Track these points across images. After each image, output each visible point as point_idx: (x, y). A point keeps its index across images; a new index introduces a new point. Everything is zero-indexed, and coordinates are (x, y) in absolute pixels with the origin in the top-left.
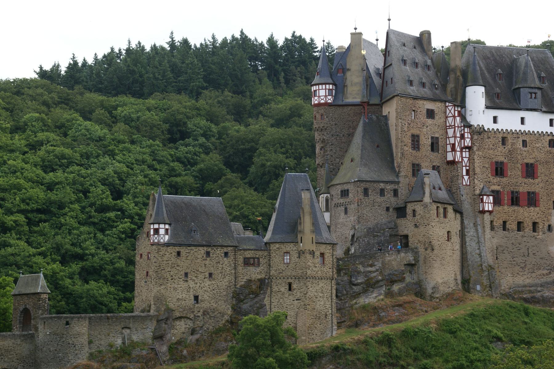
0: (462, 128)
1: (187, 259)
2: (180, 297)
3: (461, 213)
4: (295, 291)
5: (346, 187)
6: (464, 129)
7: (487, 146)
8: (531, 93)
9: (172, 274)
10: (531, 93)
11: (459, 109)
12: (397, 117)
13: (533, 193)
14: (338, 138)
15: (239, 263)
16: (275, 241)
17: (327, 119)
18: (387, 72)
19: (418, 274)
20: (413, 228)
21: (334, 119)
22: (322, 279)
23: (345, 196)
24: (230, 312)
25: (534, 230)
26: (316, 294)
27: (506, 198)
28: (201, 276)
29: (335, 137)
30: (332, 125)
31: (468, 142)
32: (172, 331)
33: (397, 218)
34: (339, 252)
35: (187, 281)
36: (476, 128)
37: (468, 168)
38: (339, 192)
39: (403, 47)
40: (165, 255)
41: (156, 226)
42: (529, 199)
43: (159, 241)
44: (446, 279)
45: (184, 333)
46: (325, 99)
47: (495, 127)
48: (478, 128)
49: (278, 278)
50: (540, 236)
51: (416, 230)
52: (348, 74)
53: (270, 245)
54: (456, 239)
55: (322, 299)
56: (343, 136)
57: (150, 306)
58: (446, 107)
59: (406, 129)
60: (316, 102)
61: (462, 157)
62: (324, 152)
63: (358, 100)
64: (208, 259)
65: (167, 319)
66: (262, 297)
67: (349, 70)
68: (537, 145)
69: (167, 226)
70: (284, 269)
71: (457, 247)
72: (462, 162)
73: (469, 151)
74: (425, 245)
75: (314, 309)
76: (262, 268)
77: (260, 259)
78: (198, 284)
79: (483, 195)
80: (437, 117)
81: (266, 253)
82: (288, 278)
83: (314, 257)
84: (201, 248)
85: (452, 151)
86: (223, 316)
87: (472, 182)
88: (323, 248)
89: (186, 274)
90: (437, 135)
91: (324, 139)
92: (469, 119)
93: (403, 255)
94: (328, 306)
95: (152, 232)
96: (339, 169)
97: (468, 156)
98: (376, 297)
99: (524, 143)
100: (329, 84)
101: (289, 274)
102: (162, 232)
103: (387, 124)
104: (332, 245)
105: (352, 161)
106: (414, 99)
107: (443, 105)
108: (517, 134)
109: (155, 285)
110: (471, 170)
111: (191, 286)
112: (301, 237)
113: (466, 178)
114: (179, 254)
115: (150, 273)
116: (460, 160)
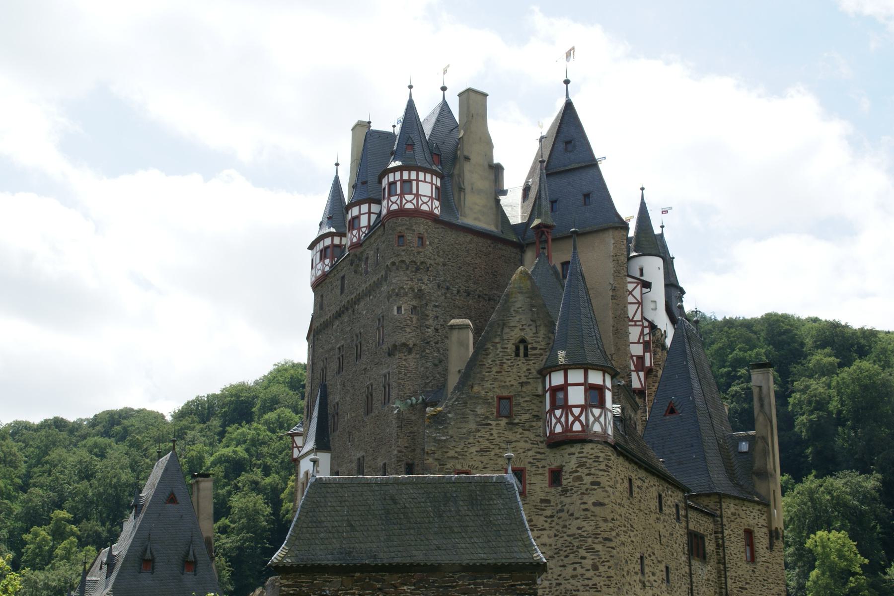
14: (448, 295)
21: (441, 253)
30: (438, 264)
36: (662, 335)
41: (595, 378)
46: (429, 203)
52: (467, 167)
53: (720, 502)
56: (458, 292)
60: (409, 206)
62: (418, 319)
77: (706, 539)
84: (652, 481)
91: (420, 290)
95: (576, 396)
112: (774, 491)
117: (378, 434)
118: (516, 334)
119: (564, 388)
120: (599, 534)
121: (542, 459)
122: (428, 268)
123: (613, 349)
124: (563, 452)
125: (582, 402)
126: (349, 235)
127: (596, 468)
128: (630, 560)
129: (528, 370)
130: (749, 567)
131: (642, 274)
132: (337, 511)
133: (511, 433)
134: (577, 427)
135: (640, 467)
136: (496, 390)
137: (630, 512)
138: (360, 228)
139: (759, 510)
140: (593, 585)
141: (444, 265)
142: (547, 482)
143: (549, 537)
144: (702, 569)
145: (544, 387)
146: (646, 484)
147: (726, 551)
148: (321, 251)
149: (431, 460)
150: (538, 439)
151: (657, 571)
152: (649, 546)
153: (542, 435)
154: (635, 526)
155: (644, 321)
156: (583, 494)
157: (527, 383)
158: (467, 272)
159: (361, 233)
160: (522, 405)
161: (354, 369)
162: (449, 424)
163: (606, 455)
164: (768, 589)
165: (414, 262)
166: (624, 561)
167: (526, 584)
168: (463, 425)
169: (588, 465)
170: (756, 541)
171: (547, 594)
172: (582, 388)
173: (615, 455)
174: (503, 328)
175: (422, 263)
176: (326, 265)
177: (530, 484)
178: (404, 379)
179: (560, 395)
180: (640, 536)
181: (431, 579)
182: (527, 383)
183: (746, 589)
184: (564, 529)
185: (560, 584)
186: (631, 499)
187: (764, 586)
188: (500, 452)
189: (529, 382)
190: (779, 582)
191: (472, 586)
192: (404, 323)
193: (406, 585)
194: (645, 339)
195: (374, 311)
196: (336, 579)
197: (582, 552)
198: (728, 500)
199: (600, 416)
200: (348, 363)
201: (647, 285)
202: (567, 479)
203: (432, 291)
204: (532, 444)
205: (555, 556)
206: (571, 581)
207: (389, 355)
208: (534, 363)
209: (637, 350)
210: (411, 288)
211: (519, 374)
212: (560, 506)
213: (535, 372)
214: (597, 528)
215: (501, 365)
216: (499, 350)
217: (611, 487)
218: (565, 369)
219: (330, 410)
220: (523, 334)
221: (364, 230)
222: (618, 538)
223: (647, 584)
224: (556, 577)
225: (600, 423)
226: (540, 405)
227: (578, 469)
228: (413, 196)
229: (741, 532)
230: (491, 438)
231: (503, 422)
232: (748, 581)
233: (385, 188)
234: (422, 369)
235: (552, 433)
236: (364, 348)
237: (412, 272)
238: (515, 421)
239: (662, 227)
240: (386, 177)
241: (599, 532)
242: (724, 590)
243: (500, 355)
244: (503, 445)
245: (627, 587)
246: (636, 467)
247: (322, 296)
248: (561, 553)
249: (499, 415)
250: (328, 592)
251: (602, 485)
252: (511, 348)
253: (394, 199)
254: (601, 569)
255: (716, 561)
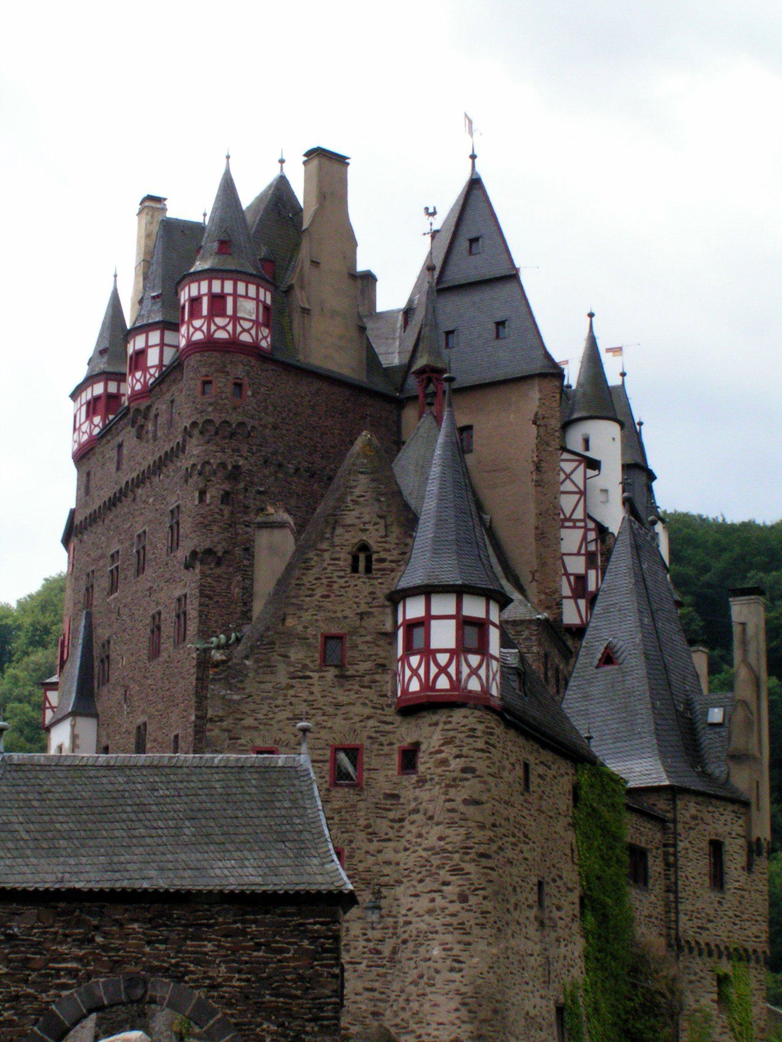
21: (271, 408)
29: (272, 469)
30: (266, 426)
40: (504, 768)
41: (474, 608)
43: (486, 690)
46: (253, 332)
49: (696, 952)
56: (297, 470)
60: (221, 335)
62: (232, 513)
76: (653, 898)
77: (650, 856)
91: (236, 467)
109: (476, 930)
117: (168, 690)
118: (351, 538)
119: (423, 623)
120: (471, 848)
121: (389, 732)
122: (249, 433)
123: (535, 564)
124: (420, 721)
125: (451, 644)
126: (130, 378)
127: (470, 747)
128: (521, 887)
129: (372, 593)
130: (715, 896)
131: (587, 448)
132: (34, 807)
133: (341, 691)
134: (443, 683)
135: (544, 746)
136: (321, 624)
137: (523, 814)
138: (145, 369)
139: (733, 812)
140: (459, 924)
141: (275, 428)
142: (396, 767)
143: (396, 851)
144: (640, 901)
145: (396, 621)
146: (553, 772)
147: (680, 873)
148: (88, 403)
149: (217, 732)
150: (382, 700)
151: (566, 904)
152: (554, 866)
153: (389, 694)
154: (530, 836)
155: (588, 521)
156: (448, 786)
157: (369, 614)
158: (311, 439)
159: (148, 376)
160: (360, 648)
161: (134, 588)
162: (246, 676)
163: (487, 727)
164: (740, 929)
165: (225, 422)
166: (510, 888)
167: (322, 923)
168: (266, 678)
169: (458, 743)
170: (726, 858)
171: (390, 938)
172: (452, 623)
173: (502, 727)
174: (334, 528)
175: (241, 424)
176: (96, 426)
177: (369, 770)
178: (207, 606)
179: (418, 633)
180: (539, 850)
181: (176, 913)
182: (369, 614)
183: (708, 929)
184: (419, 840)
185: (410, 923)
186: (526, 794)
187: (735, 924)
188: (324, 721)
189: (372, 613)
190: (758, 918)
191: (239, 925)
192: (210, 518)
193: (137, 921)
194: (589, 549)
195: (165, 499)
196: (31, 912)
197: (444, 875)
198: (687, 797)
199: (479, 666)
200: (125, 579)
201: (594, 464)
202: (425, 763)
203: (254, 469)
204: (374, 708)
205: (405, 880)
206: (426, 918)
207: (187, 567)
208: (381, 583)
209: (577, 565)
210: (221, 463)
211: (357, 600)
212: (413, 805)
213: (382, 600)
214: (468, 838)
215: (330, 585)
216: (327, 562)
217: (493, 776)
218: (427, 591)
219: (97, 651)
220: (364, 538)
221: (152, 371)
222: (502, 854)
223: (547, 922)
224: (404, 912)
225: (479, 678)
226: (388, 647)
227: (443, 748)
228: (227, 320)
229: (705, 845)
230: (310, 698)
231: (331, 673)
232: (711, 918)
233: (183, 308)
234: (237, 590)
235: (405, 691)
236: (149, 556)
237: (224, 438)
238: (349, 673)
239: (623, 375)
240: (187, 289)
241: (472, 845)
242: (673, 932)
243: (328, 571)
244: (330, 710)
245: (514, 927)
246: (536, 746)
247: (88, 474)
248: (413, 874)
249: (325, 662)
250: (16, 930)
251: (477, 773)
252: (345, 560)
253: (197, 323)
254: (473, 900)
255: (664, 888)
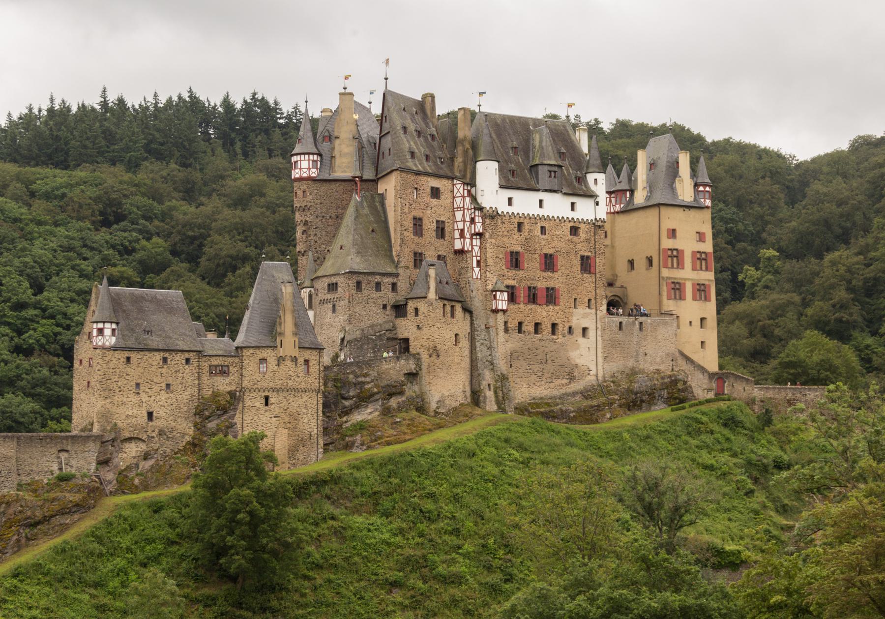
0: (473, 210)
1: (138, 367)
2: (130, 414)
3: (471, 312)
4: (273, 407)
5: (334, 280)
6: (474, 212)
7: (501, 233)
8: (550, 172)
9: (119, 385)
10: (550, 172)
11: (469, 188)
12: (396, 196)
13: (552, 289)
15: (204, 371)
16: (249, 345)
17: (310, 196)
18: (383, 141)
19: (421, 385)
20: (415, 330)
22: (306, 391)
23: (333, 290)
24: (191, 432)
25: (553, 333)
26: (299, 410)
27: (522, 295)
28: (156, 388)
31: (479, 228)
32: (120, 454)
33: (396, 317)
34: (326, 360)
35: (138, 393)
37: (478, 258)
38: (326, 286)
39: (403, 113)
41: (100, 326)
42: (547, 295)
43: (104, 344)
44: (453, 391)
45: (134, 458)
47: (510, 210)
48: (491, 211)
49: (252, 390)
50: (559, 338)
51: (418, 332)
52: (337, 143)
54: (465, 343)
55: (305, 416)
56: (330, 217)
57: (92, 424)
58: (454, 185)
59: (406, 210)
60: (297, 176)
61: (472, 246)
63: (348, 175)
64: (165, 366)
65: (113, 440)
66: (232, 413)
67: (337, 138)
68: (557, 233)
69: (114, 326)
70: (259, 379)
71: (467, 352)
72: (472, 251)
73: (480, 239)
74: (429, 350)
75: (296, 428)
78: (153, 398)
79: (496, 291)
80: (442, 197)
81: (237, 360)
82: (264, 391)
83: (296, 365)
84: (156, 354)
85: (460, 238)
86: (183, 437)
87: (483, 275)
88: (307, 354)
89: (138, 385)
90: (442, 219)
92: (480, 200)
93: (403, 362)
94: (313, 424)
95: (95, 333)
96: (324, 258)
97: (478, 244)
98: (371, 413)
99: (543, 228)
100: (313, 154)
101: (266, 385)
102: (108, 332)
103: (383, 204)
104: (318, 351)
105: (341, 248)
106: (417, 174)
107: (450, 182)
108: (534, 219)
110: (482, 261)
111: (144, 400)
113: (477, 270)
114: (128, 359)
115: (92, 384)
116: (470, 249)
141: (321, 203)
175: (306, 206)
